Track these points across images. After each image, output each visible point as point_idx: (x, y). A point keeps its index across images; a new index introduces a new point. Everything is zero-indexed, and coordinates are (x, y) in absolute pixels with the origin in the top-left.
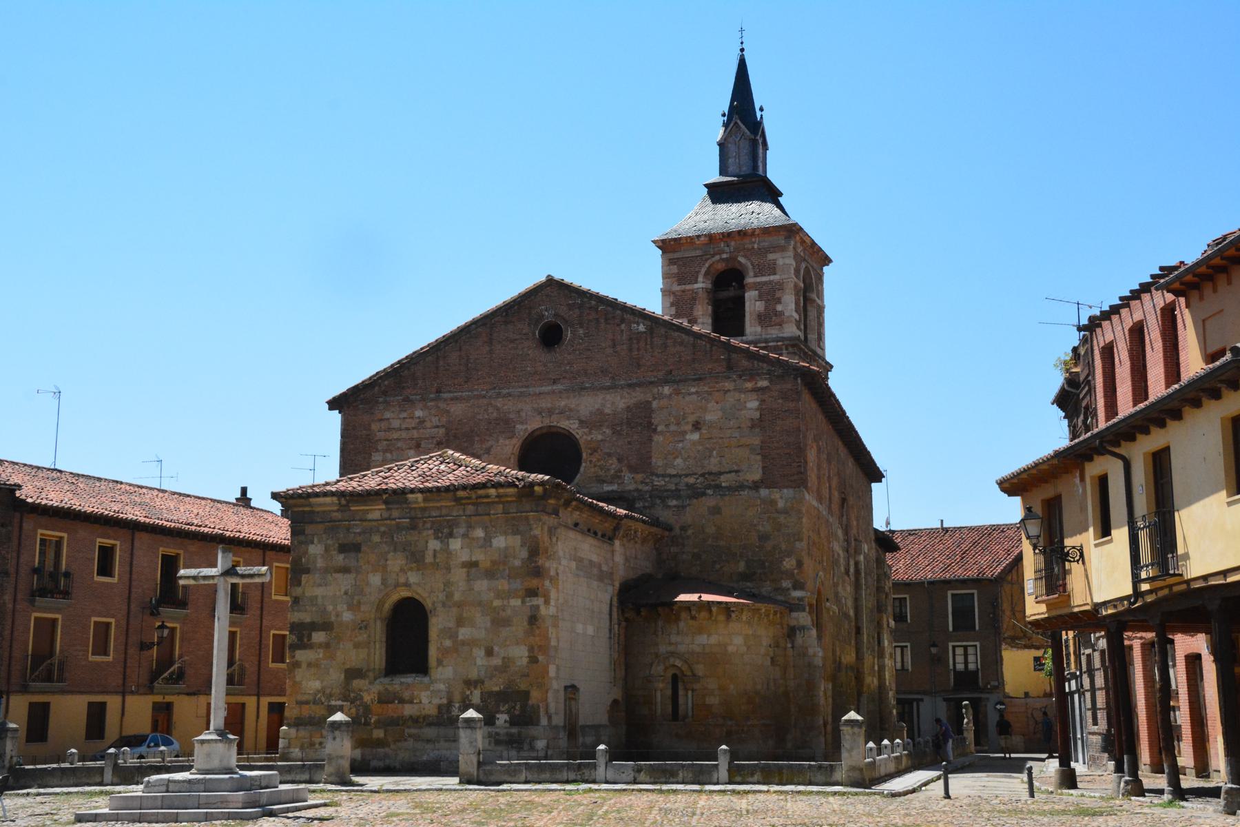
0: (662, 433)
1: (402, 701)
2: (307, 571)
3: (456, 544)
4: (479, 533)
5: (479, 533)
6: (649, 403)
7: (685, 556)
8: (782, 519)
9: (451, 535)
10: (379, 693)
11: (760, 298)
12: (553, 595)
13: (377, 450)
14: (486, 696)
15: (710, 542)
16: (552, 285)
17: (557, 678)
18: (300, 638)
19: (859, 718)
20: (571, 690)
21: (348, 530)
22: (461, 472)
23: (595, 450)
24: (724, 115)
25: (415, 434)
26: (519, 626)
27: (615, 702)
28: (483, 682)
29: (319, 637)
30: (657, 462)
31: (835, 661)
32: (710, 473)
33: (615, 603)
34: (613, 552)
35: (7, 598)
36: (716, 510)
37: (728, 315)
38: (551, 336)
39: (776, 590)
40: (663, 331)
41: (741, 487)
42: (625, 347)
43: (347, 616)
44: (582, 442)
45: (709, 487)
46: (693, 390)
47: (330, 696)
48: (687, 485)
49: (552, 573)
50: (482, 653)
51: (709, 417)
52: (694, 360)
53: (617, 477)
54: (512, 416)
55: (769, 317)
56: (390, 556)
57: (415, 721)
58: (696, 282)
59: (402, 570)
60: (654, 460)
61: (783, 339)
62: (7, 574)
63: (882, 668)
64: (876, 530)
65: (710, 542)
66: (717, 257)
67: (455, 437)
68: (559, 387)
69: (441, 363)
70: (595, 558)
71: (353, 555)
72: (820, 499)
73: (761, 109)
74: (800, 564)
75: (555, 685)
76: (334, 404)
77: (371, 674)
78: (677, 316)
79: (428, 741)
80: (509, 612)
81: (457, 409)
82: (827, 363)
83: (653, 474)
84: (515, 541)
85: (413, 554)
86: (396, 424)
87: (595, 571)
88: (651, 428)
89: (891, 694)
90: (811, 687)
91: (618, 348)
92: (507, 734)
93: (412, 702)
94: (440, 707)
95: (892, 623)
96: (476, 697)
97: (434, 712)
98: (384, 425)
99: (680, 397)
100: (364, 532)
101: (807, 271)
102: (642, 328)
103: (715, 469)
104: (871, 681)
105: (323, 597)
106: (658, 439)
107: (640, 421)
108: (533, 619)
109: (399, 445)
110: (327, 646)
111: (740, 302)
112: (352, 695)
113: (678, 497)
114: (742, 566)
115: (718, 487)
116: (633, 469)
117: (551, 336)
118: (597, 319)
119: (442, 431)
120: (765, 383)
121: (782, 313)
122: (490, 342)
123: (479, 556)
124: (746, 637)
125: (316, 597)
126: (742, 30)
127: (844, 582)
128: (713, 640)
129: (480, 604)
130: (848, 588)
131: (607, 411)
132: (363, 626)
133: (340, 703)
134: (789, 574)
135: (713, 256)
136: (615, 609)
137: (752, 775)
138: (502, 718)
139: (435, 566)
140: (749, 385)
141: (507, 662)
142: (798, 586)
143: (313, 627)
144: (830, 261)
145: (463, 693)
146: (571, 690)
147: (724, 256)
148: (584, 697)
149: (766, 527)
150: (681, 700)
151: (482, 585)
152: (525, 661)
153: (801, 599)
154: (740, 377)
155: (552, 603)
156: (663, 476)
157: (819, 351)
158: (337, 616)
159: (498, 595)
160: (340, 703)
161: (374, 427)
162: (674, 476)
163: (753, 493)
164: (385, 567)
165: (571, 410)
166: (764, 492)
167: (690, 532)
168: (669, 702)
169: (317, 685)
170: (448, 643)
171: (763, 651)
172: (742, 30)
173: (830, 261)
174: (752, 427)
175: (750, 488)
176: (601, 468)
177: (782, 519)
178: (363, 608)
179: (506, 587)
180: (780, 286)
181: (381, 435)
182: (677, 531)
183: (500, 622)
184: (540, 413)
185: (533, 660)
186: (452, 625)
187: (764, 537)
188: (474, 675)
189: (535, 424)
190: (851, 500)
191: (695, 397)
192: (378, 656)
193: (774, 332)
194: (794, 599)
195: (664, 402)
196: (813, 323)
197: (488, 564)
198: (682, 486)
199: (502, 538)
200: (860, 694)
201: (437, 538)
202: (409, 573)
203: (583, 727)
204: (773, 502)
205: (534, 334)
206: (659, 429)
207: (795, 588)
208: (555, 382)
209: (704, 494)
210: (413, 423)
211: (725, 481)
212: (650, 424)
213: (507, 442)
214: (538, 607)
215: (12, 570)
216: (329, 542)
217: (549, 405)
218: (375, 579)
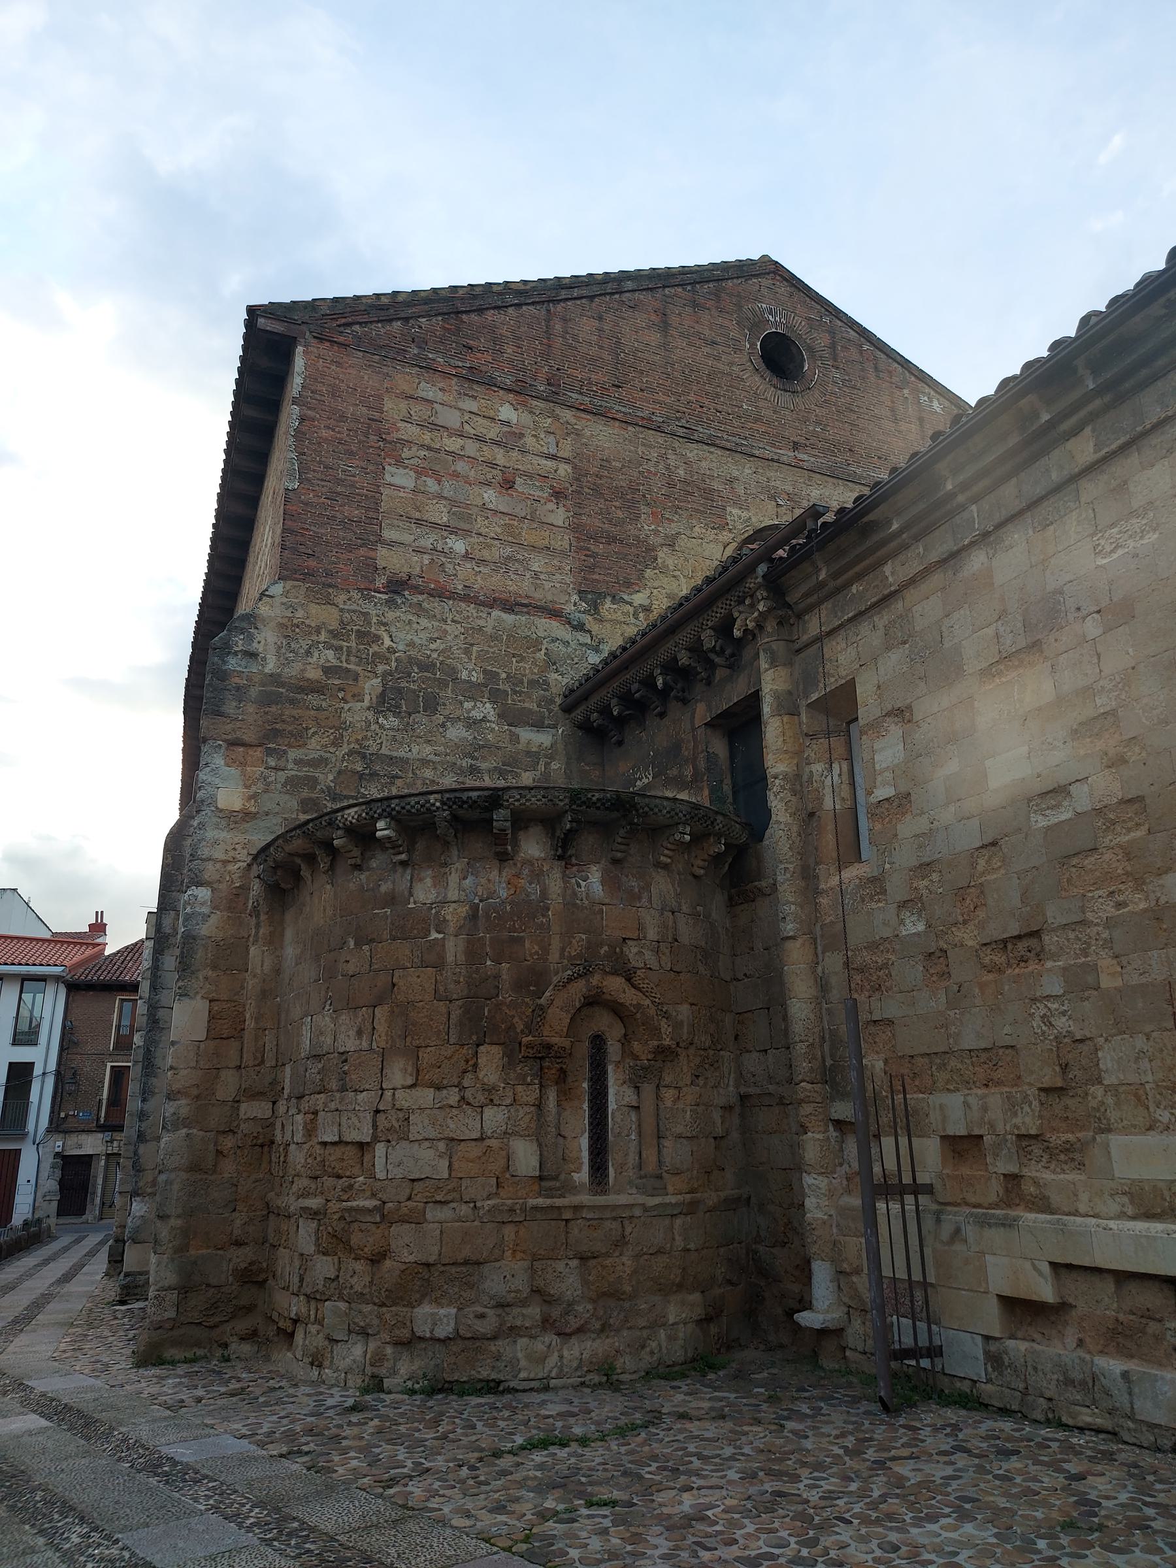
25: (500, 457)
54: (716, 485)
67: (597, 491)
69: (558, 327)
86: (451, 418)
98: (419, 411)
109: (461, 466)
119: (564, 470)
161: (388, 404)
181: (410, 431)
184: (773, 498)
205: (753, 345)
213: (711, 535)
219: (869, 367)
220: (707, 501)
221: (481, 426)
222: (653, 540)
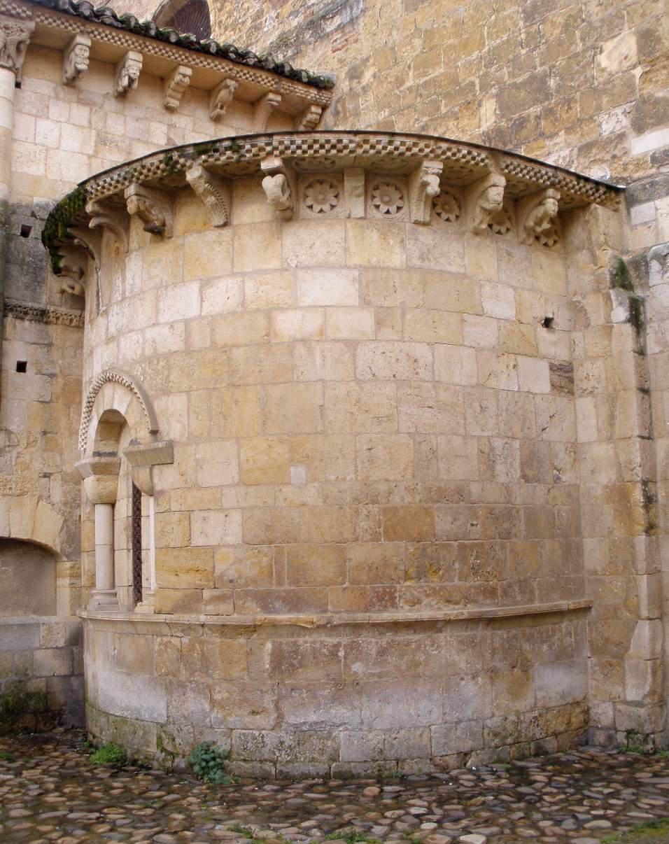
124: (370, 279)
128: (223, 295)
167: (368, 76)
168: (123, 541)
182: (343, 86)
194: (639, 164)
207: (640, 127)
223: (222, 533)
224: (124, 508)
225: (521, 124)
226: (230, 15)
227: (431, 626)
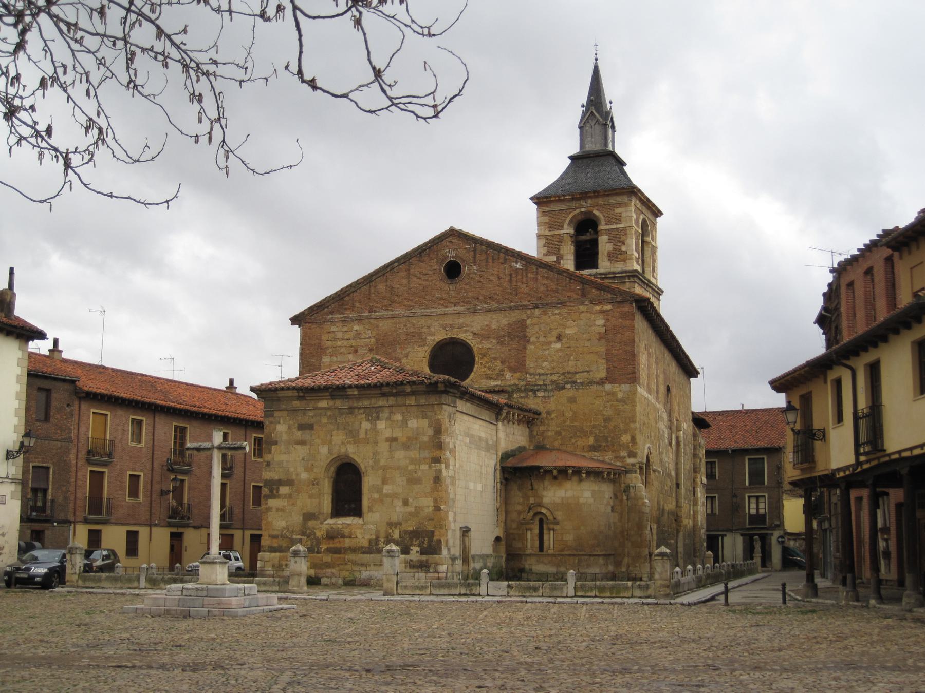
0: (534, 343)
1: (343, 537)
2: (276, 443)
3: (381, 425)
4: (398, 417)
5: (398, 417)
6: (524, 321)
7: (550, 434)
8: (620, 406)
9: (378, 418)
10: (327, 532)
11: (610, 241)
12: (451, 462)
13: (326, 354)
14: (403, 533)
15: (568, 423)
16: (453, 234)
17: (455, 521)
18: (271, 491)
19: (668, 551)
20: (466, 531)
21: (304, 414)
22: (386, 373)
23: (484, 355)
24: (583, 106)
25: (353, 342)
26: (428, 484)
27: (498, 539)
28: (400, 524)
29: (284, 490)
30: (530, 364)
31: (659, 509)
32: (569, 373)
33: (498, 467)
34: (497, 430)
35: (72, 456)
36: (572, 400)
37: (586, 255)
38: (453, 270)
39: (616, 457)
40: (534, 268)
41: (591, 383)
42: (507, 279)
43: (304, 476)
44: (475, 349)
45: (567, 383)
46: (556, 311)
47: (293, 532)
48: (551, 381)
49: (451, 446)
50: (400, 503)
51: (568, 331)
52: (557, 290)
53: (500, 375)
55: (617, 255)
56: (334, 432)
57: (354, 550)
58: (562, 229)
59: (343, 443)
60: (528, 363)
61: (626, 272)
62: (70, 440)
63: (695, 513)
64: (693, 413)
65: (568, 423)
66: (578, 211)
67: (383, 345)
68: (458, 308)
69: (373, 291)
70: (483, 435)
71: (308, 431)
72: (649, 392)
73: (611, 103)
74: (633, 439)
75: (452, 526)
76: (295, 320)
77: (321, 517)
78: (549, 253)
79: (362, 565)
80: (420, 474)
81: (384, 325)
82: (659, 289)
83: (527, 373)
84: (425, 422)
85: (351, 431)
86: (339, 335)
87: (483, 444)
88: (525, 339)
89: (703, 531)
90: (640, 527)
91: (502, 280)
92: (418, 561)
93: (350, 537)
94: (370, 541)
95: (705, 480)
96: (396, 536)
97: (366, 544)
98: (331, 336)
99: (547, 317)
100: (315, 415)
101: (644, 221)
102: (519, 266)
103: (572, 370)
104: (688, 523)
105: (287, 462)
106: (530, 347)
107: (518, 335)
108: (437, 479)
110: (290, 496)
111: (595, 243)
112: (308, 532)
113: (545, 390)
114: (591, 441)
115: (575, 382)
116: (513, 370)
117: (453, 270)
118: (487, 259)
119: (373, 340)
120: (609, 307)
121: (625, 252)
122: (408, 276)
123: (398, 433)
124: (593, 492)
125: (282, 462)
126: (596, 45)
127: (667, 451)
128: (570, 494)
129: (399, 468)
130: (671, 456)
131: (494, 326)
132: (315, 483)
133: (299, 537)
134: (625, 447)
135: (575, 209)
136: (498, 472)
137: (592, 590)
138: (415, 549)
139: (366, 441)
140: (598, 308)
141: (418, 510)
142: (632, 455)
143: (280, 483)
144: (662, 214)
145: (387, 531)
146: (466, 531)
147: (583, 210)
148: (472, 534)
149: (609, 412)
150: (545, 537)
151: (400, 454)
152: (431, 509)
153: (633, 465)
154: (591, 302)
155: (451, 467)
156: (535, 375)
157: (653, 281)
158: (297, 475)
159: (413, 461)
160: (299, 537)
161: (324, 337)
162: (543, 374)
163: (600, 387)
164: (331, 442)
165: (467, 326)
166: (608, 387)
167: (553, 416)
168: (537, 538)
169: (283, 524)
170: (376, 496)
171: (605, 501)
172: (596, 45)
173: (662, 214)
174: (599, 339)
175: (598, 383)
176: (489, 368)
177: (620, 406)
178: (315, 470)
179: (418, 456)
180: (624, 232)
181: (329, 343)
182: (544, 415)
183: (413, 481)
184: (444, 328)
185: (437, 509)
186: (379, 482)
187: (607, 420)
188: (395, 518)
189: (440, 336)
190: (674, 391)
191: (557, 316)
192: (327, 504)
193: (619, 267)
195: (535, 320)
196: (649, 260)
197: (405, 439)
198: (547, 383)
199: (415, 421)
200: (678, 532)
201: (368, 420)
202: (348, 445)
203: (473, 557)
204: (614, 394)
205: (440, 270)
206: (532, 339)
207: (629, 456)
208: (455, 306)
209: (563, 388)
210: (351, 335)
211: (579, 378)
212: (525, 336)
213: (420, 349)
214: (440, 471)
215: (74, 437)
216: (291, 422)
217: (451, 323)
218: (324, 450)
219: (490, 260)
220: (418, 336)
221: (348, 335)
222: (401, 356)
223: (569, 538)
224: (537, 531)
225: (600, 446)
226: (487, 363)
227: (599, 556)
